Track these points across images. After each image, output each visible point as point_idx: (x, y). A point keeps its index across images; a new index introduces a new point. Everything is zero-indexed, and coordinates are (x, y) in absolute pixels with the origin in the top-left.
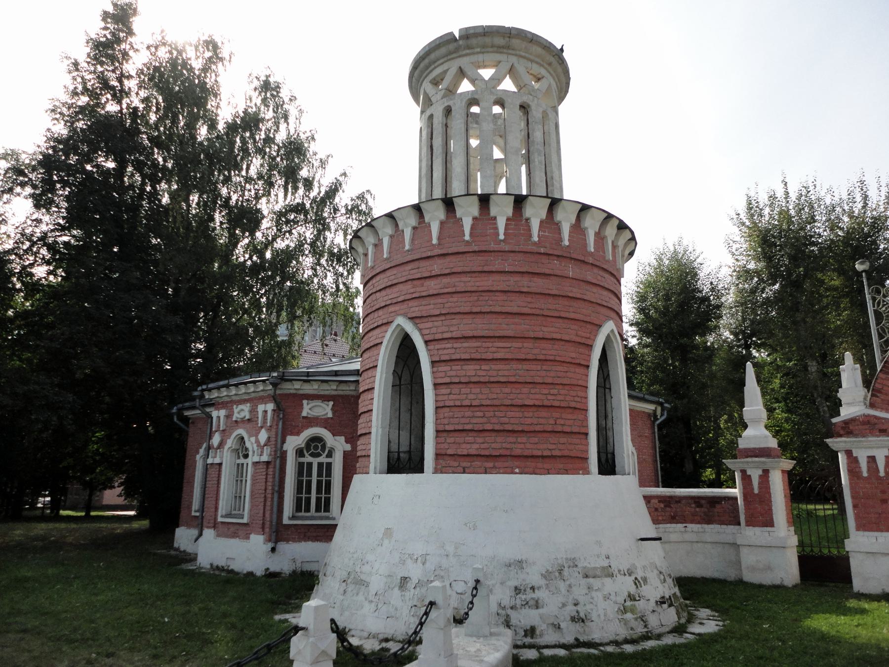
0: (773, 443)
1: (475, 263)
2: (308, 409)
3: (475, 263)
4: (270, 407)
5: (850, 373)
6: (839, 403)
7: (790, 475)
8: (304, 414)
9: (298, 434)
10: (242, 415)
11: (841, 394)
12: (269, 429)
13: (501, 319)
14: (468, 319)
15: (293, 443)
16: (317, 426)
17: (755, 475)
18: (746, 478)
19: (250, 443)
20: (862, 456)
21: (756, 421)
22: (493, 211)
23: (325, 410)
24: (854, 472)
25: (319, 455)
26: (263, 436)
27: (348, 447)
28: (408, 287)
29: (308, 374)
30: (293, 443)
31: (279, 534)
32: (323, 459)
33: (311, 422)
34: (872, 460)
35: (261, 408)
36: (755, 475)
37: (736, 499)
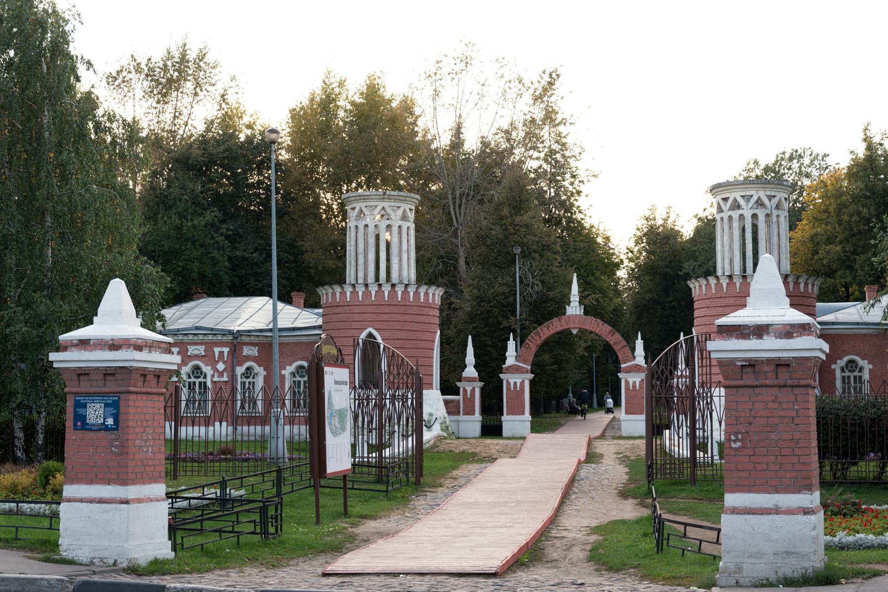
0: (476, 375)
1: (401, 310)
2: (247, 351)
3: (401, 310)
4: (226, 350)
5: (511, 344)
6: (505, 359)
7: (482, 390)
8: (244, 354)
9: (241, 365)
10: (196, 352)
11: (507, 354)
12: (224, 362)
13: (411, 333)
14: (399, 332)
15: (240, 370)
16: (250, 360)
17: (469, 389)
18: (465, 391)
19: (207, 370)
20: (512, 382)
21: (470, 365)
22: (409, 289)
23: (253, 351)
24: (508, 389)
25: (247, 377)
26: (221, 366)
27: (265, 373)
28: (373, 316)
29: (249, 331)
30: (240, 370)
31: (235, 422)
32: (250, 380)
33: (248, 358)
34: (515, 383)
35: (217, 350)
36: (469, 389)
37: (459, 401)
